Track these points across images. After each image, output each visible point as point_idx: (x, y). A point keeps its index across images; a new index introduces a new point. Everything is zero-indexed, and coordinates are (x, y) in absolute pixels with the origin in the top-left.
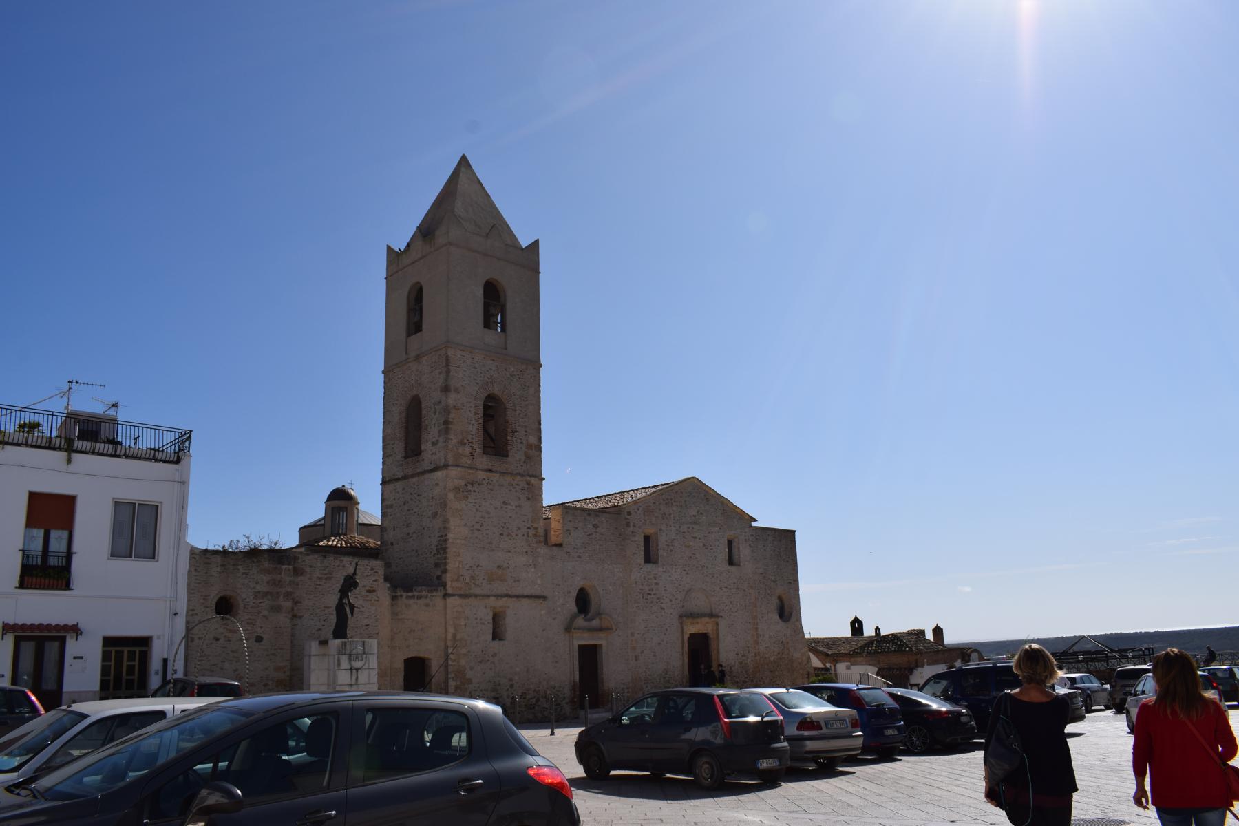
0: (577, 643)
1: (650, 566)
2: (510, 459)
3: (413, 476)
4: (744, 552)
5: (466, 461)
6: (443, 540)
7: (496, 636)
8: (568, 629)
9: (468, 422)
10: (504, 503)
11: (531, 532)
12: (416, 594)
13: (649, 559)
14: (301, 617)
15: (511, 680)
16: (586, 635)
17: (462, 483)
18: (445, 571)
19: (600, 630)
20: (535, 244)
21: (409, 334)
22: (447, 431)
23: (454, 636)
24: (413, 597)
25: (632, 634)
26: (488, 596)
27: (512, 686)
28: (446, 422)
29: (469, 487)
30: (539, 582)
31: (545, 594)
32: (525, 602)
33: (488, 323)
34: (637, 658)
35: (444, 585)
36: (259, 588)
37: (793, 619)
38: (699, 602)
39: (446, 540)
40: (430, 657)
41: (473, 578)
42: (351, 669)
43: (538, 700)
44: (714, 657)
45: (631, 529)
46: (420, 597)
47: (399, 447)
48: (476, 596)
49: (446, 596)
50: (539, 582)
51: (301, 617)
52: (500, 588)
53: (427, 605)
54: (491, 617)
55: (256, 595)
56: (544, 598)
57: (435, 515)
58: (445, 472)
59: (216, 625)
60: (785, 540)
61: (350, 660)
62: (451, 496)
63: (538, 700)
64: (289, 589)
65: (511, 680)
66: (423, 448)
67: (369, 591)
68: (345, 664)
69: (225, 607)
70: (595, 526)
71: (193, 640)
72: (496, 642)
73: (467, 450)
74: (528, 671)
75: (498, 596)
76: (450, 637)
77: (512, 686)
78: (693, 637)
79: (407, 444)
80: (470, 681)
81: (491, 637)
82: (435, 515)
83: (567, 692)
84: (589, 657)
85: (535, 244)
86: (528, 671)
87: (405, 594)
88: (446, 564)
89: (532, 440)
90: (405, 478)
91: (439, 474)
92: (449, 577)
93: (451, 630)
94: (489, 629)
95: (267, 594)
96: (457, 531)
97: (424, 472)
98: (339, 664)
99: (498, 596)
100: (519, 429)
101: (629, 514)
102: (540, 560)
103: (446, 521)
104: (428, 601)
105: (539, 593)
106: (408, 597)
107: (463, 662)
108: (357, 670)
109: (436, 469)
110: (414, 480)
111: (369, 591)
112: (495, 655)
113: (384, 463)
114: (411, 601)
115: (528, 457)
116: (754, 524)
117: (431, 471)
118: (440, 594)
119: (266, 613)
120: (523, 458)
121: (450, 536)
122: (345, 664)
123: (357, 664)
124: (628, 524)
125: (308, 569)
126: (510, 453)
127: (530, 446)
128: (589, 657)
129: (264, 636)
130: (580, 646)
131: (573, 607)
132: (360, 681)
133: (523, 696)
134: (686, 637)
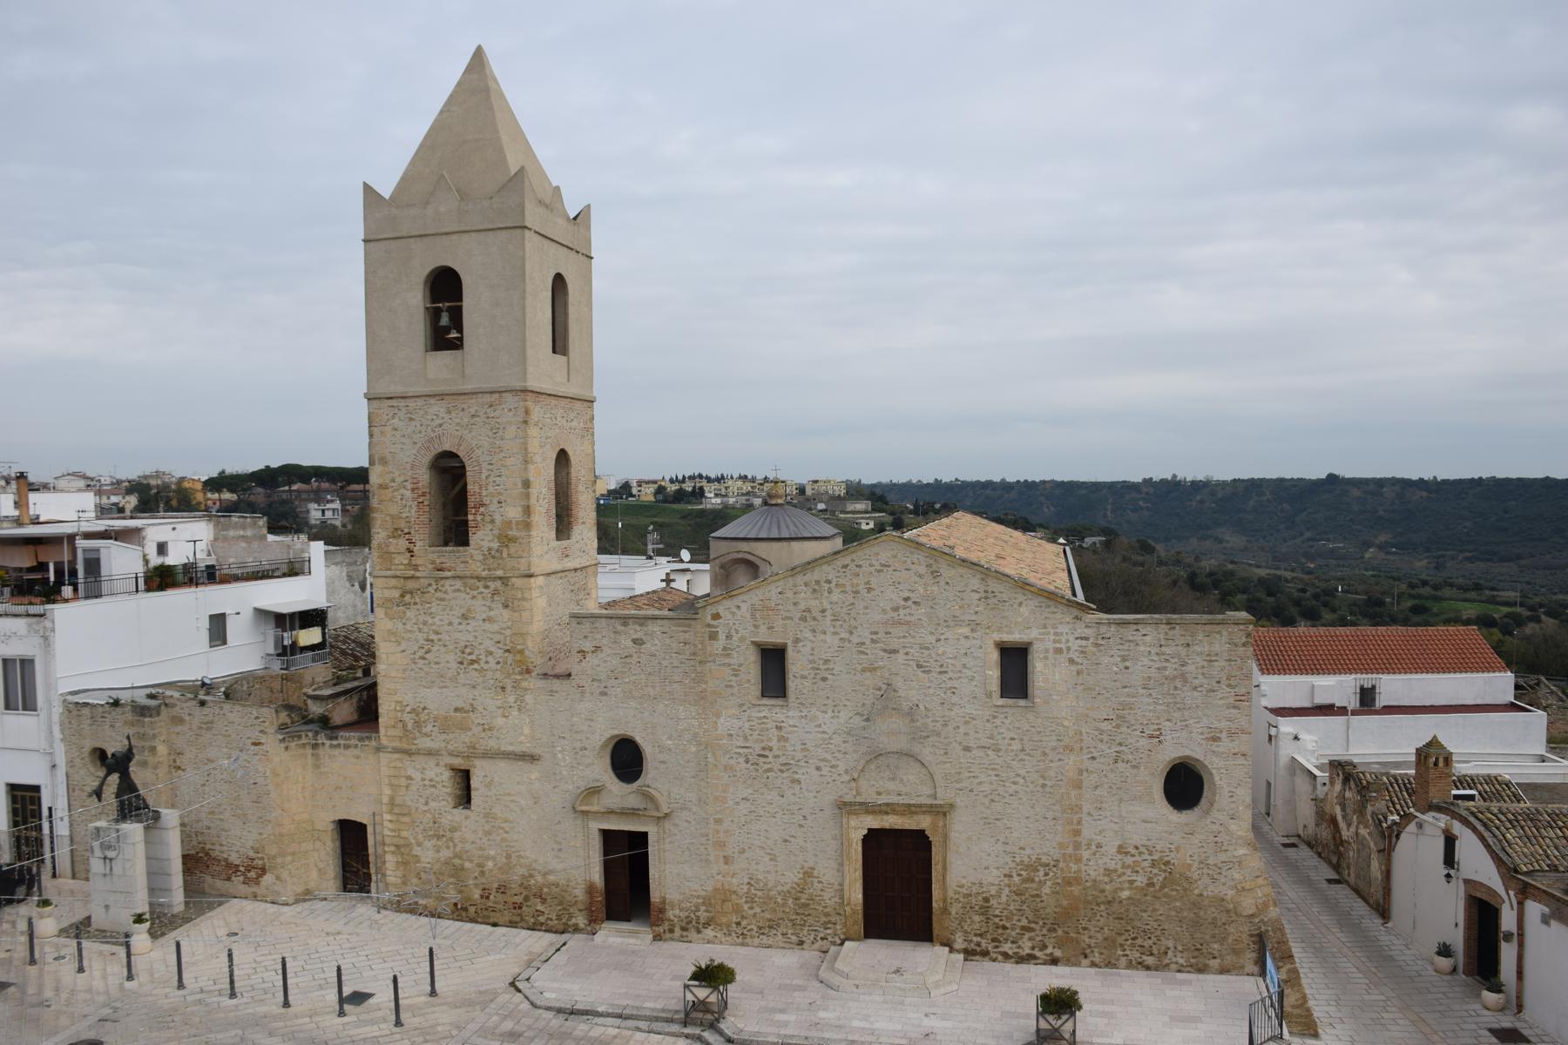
0: (596, 826)
2: (470, 550)
15: (480, 865)
17: (396, 594)
23: (392, 799)
25: (718, 821)
27: (482, 873)
31: (537, 751)
32: (503, 765)
41: (418, 724)
43: (527, 899)
46: (347, 747)
49: (378, 749)
50: (527, 731)
52: (460, 740)
53: (358, 757)
56: (532, 758)
63: (527, 899)
65: (480, 865)
68: (98, 853)
73: (403, 543)
74: (508, 857)
76: (385, 800)
80: (417, 859)
83: (580, 893)
87: (328, 743)
100: (486, 500)
102: (529, 698)
104: (357, 752)
106: (331, 746)
107: (404, 834)
112: (453, 830)
114: (336, 752)
115: (506, 540)
120: (495, 545)
123: (111, 854)
124: (713, 636)
125: (187, 718)
131: (601, 770)
134: (858, 835)
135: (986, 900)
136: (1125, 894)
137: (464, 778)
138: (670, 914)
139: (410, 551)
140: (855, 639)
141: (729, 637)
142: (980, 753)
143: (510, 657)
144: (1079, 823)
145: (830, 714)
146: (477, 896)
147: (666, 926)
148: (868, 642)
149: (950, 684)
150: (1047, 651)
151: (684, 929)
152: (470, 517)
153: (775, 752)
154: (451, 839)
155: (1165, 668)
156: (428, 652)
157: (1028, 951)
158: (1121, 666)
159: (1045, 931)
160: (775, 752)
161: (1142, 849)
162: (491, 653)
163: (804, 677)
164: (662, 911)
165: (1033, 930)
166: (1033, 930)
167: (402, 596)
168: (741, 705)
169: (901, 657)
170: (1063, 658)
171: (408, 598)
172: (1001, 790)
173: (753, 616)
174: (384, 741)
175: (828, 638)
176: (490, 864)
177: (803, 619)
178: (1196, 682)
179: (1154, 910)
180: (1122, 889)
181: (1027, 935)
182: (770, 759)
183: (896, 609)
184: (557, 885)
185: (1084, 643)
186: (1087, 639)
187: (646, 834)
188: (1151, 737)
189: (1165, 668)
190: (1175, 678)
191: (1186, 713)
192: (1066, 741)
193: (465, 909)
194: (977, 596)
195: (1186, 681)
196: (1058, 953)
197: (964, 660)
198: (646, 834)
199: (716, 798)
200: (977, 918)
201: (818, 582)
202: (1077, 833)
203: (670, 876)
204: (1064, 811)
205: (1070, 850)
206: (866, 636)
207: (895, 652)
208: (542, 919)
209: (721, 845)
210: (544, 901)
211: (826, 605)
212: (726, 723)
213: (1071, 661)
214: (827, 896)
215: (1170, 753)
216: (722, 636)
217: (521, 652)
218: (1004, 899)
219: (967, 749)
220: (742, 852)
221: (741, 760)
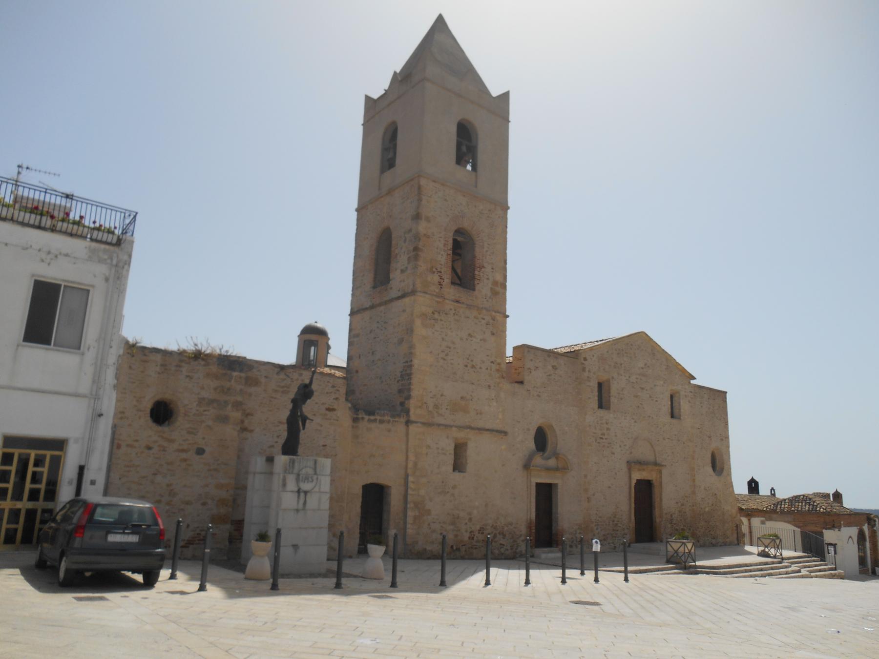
1: (602, 412)
2: (476, 293)
3: (380, 305)
4: (685, 406)
5: (435, 289)
6: (408, 366)
7: (458, 466)
8: (527, 466)
9: (439, 252)
10: (469, 335)
11: (494, 367)
12: (378, 418)
13: (603, 404)
14: (252, 431)
15: (470, 514)
18: (409, 397)
19: (557, 469)
20: (505, 96)
21: (383, 171)
22: (416, 258)
23: (415, 464)
24: (375, 420)
25: (586, 476)
26: (451, 426)
27: (470, 519)
28: (416, 249)
29: (436, 316)
30: (500, 416)
33: (460, 160)
34: (589, 500)
35: (407, 412)
36: (205, 394)
37: (725, 473)
39: (411, 366)
40: (390, 484)
41: (436, 406)
42: (299, 492)
43: (495, 536)
44: (657, 504)
45: (586, 374)
46: (381, 422)
47: (369, 278)
48: (439, 425)
50: (500, 416)
51: (252, 431)
53: (389, 431)
54: (451, 449)
55: (201, 401)
56: (505, 433)
57: (401, 341)
58: (412, 298)
59: (150, 432)
60: (719, 397)
61: (298, 480)
62: (418, 323)
63: (495, 536)
64: (239, 399)
65: (470, 514)
66: (391, 276)
67: (328, 409)
68: (291, 485)
69: (162, 413)
70: (554, 367)
71: (119, 447)
72: (457, 474)
73: (436, 278)
74: (486, 505)
75: (460, 428)
77: (470, 519)
78: (639, 482)
79: (376, 274)
80: (429, 512)
81: (451, 468)
82: (401, 341)
83: (523, 530)
84: (545, 495)
85: (505, 96)
87: (367, 417)
88: (409, 390)
89: (499, 278)
90: (372, 307)
91: (407, 300)
92: (412, 404)
93: (412, 458)
94: (450, 459)
95: (211, 402)
96: (422, 358)
97: (392, 300)
98: (284, 485)
99: (460, 428)
100: (485, 265)
101: (585, 359)
103: (412, 347)
105: (499, 427)
106: (369, 421)
107: (422, 492)
108: (306, 493)
109: (403, 296)
110: (382, 308)
111: (328, 409)
112: (454, 487)
113: (353, 295)
114: (373, 425)
115: (495, 293)
116: (692, 382)
117: (399, 298)
118: (403, 420)
119: (210, 423)
120: (489, 294)
121: (416, 362)
122: (291, 485)
123: (305, 486)
124: (584, 369)
125: (263, 380)
126: (477, 287)
127: (495, 283)
128: (545, 495)
129: (207, 449)
130: (539, 486)
131: (532, 445)
132: (309, 505)
133: (481, 530)
134: (634, 482)
137: (460, 450)
139: (440, 284)
143: (494, 367)
146: (466, 539)
151: (571, 546)
152: (476, 273)
154: (453, 495)
156: (447, 355)
162: (483, 362)
167: (433, 313)
171: (436, 316)
174: (413, 417)
176: (475, 512)
177: (615, 367)
184: (511, 524)
193: (458, 549)
202: (694, 480)
203: (568, 514)
208: (502, 550)
210: (504, 536)
217: (499, 364)
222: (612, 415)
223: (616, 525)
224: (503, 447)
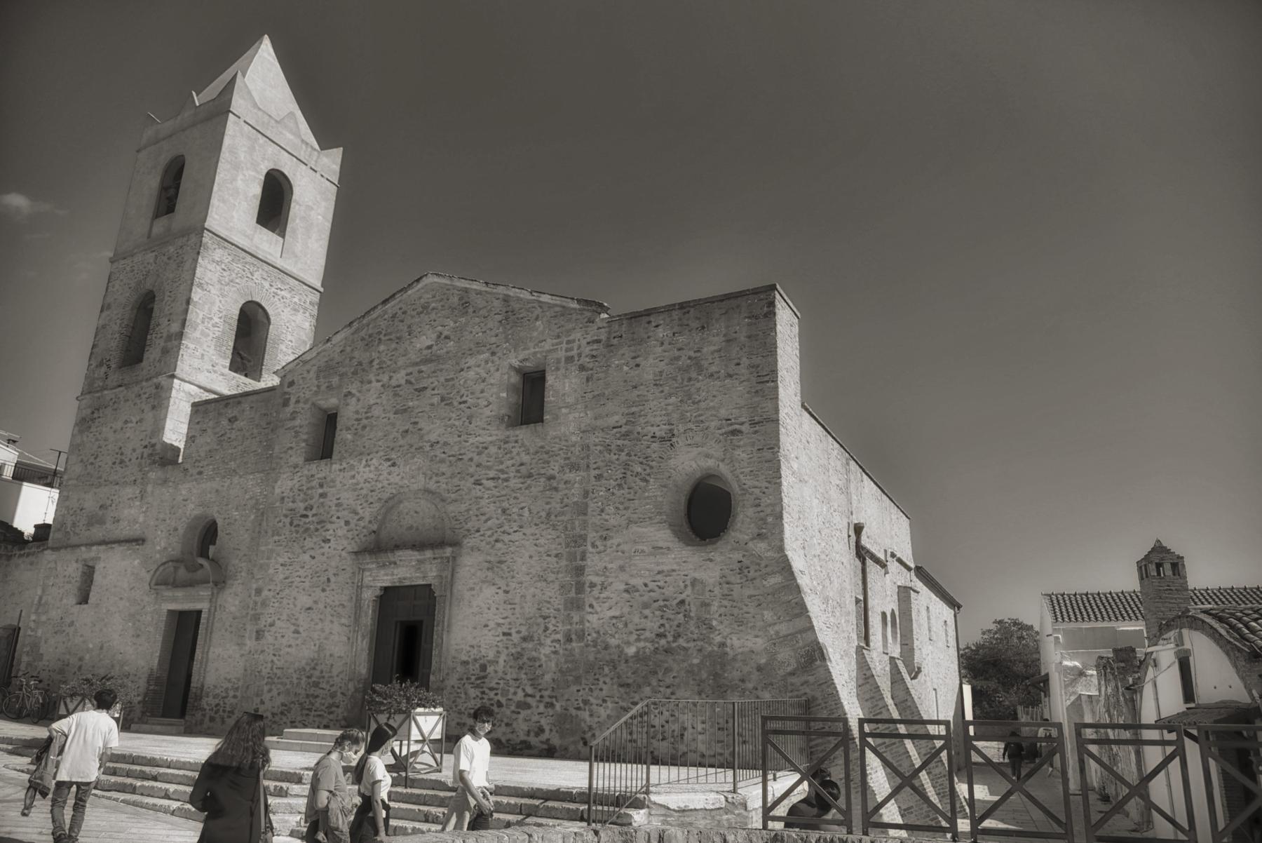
11: (147, 452)
16: (179, 593)
17: (89, 411)
25: (259, 591)
27: (80, 668)
30: (141, 519)
34: (259, 635)
38: (417, 514)
45: (290, 409)
65: (81, 659)
70: (232, 420)
74: (101, 648)
84: (185, 632)
86: (101, 648)
102: (149, 488)
128: (185, 632)
134: (369, 595)
135: (483, 668)
136: (631, 651)
138: (204, 702)
140: (394, 382)
141: (298, 402)
142: (491, 484)
144: (583, 559)
145: (364, 462)
147: (199, 715)
148: (403, 382)
149: (468, 412)
150: (558, 361)
153: (314, 511)
155: (678, 358)
157: (523, 737)
158: (632, 363)
159: (542, 708)
160: (314, 511)
161: (652, 585)
163: (348, 429)
164: (199, 698)
165: (528, 706)
166: (528, 706)
168: (296, 466)
169: (429, 392)
170: (573, 368)
171: (96, 415)
172: (506, 528)
173: (318, 378)
175: (374, 384)
176: (87, 657)
178: (713, 369)
179: (668, 670)
180: (628, 643)
181: (524, 713)
182: (310, 519)
183: (429, 347)
185: (595, 346)
186: (598, 341)
187: (199, 612)
188: (662, 440)
189: (678, 358)
190: (686, 369)
191: (703, 405)
192: (573, 459)
194: (499, 317)
195: (700, 369)
196: (556, 741)
197: (482, 386)
198: (199, 612)
199: (261, 567)
200: (473, 692)
201: (370, 336)
202: (580, 571)
204: (567, 546)
205: (573, 594)
206: (400, 377)
207: (425, 388)
209: (256, 618)
211: (374, 355)
212: (285, 484)
213: (582, 368)
214: (335, 672)
215: (688, 462)
216: (293, 400)
218: (501, 661)
219: (478, 483)
220: (271, 625)
221: (288, 520)
222: (336, 467)
223: (316, 684)
224: (136, 562)
